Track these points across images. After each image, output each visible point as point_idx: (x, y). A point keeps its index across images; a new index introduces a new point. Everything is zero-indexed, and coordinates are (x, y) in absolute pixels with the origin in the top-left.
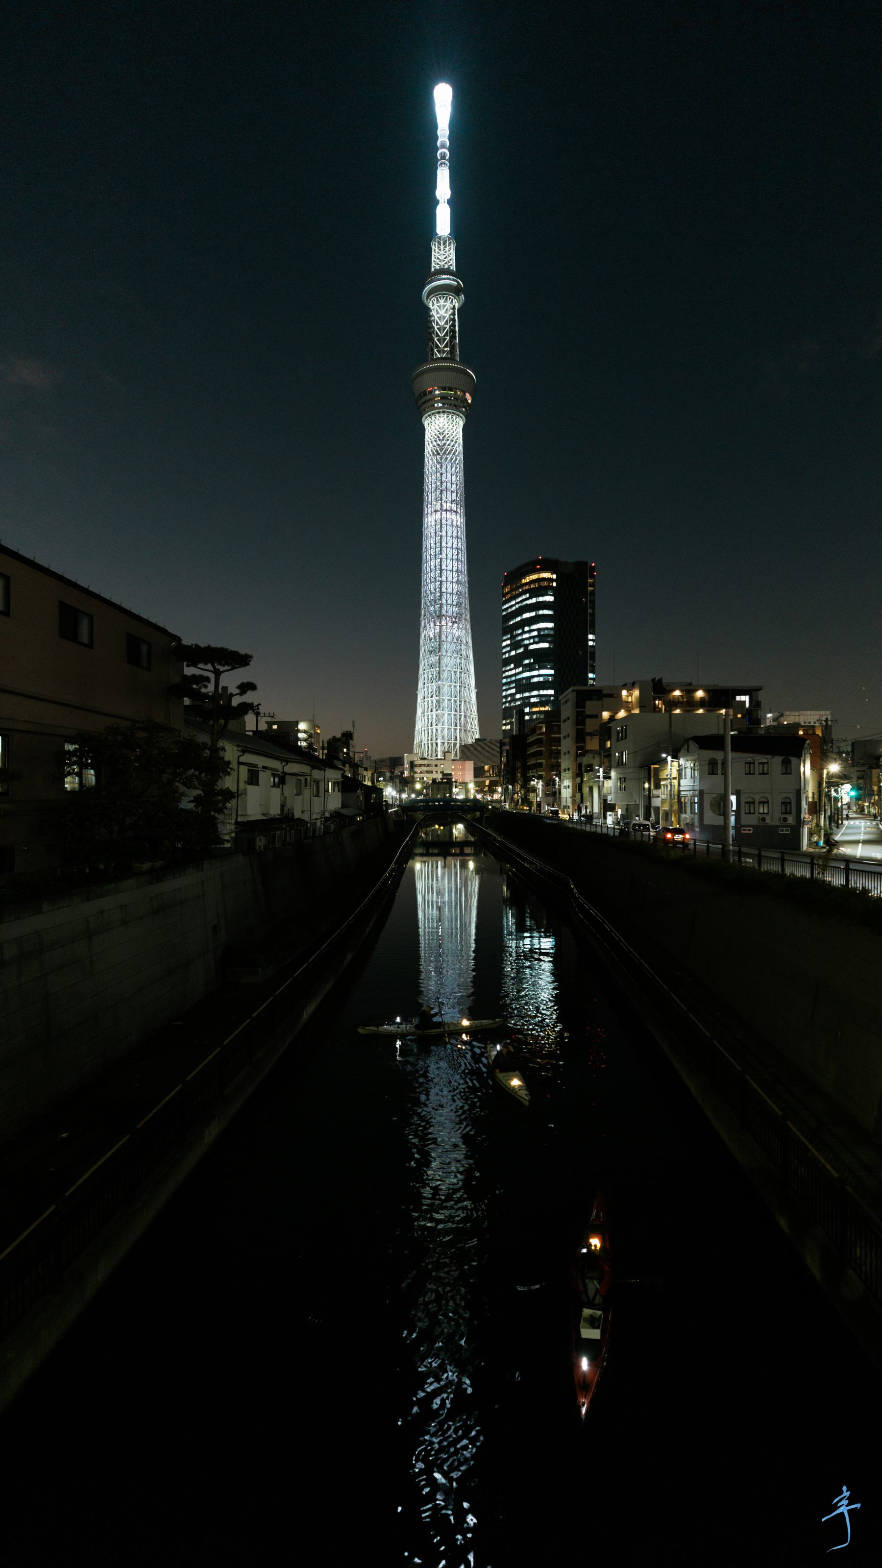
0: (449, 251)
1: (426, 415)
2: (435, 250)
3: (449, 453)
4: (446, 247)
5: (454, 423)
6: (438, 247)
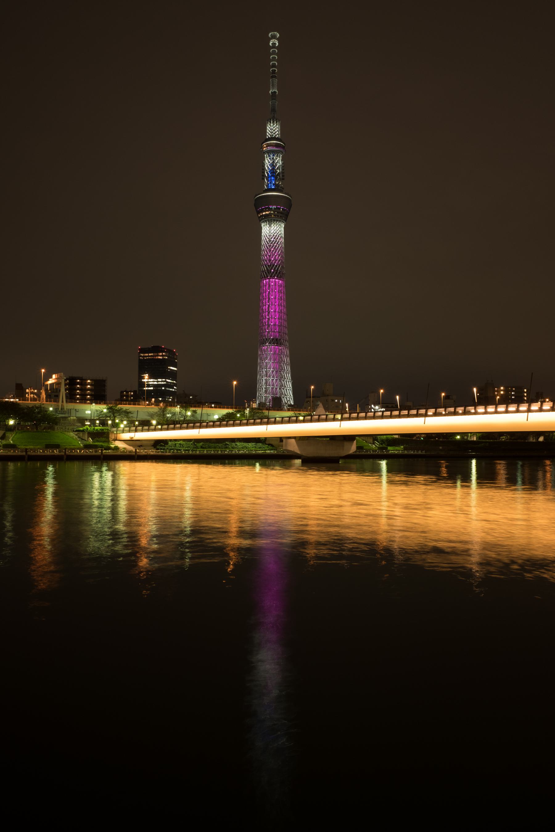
0: (276, 126)
1: (262, 221)
2: (268, 126)
3: (274, 243)
4: (274, 124)
5: (278, 226)
6: (270, 125)
